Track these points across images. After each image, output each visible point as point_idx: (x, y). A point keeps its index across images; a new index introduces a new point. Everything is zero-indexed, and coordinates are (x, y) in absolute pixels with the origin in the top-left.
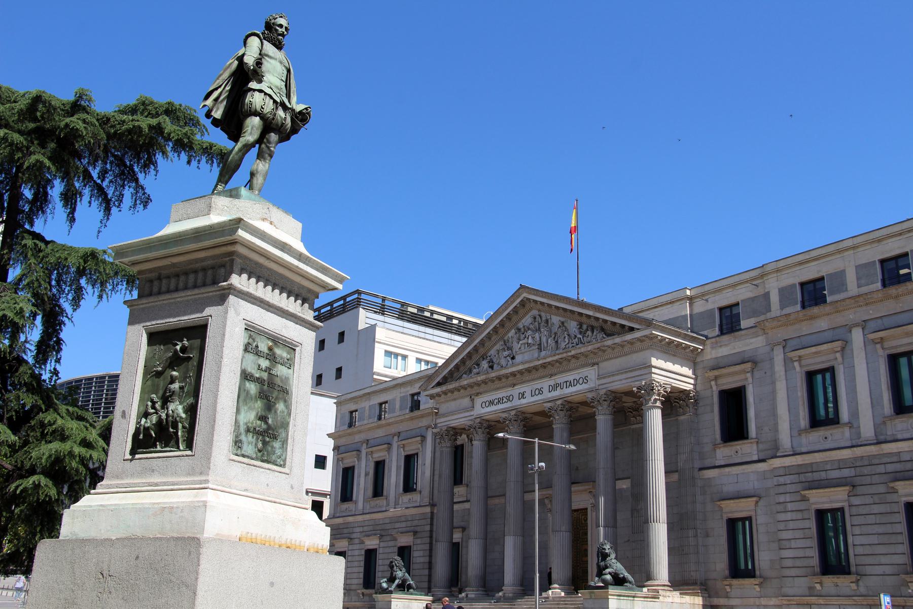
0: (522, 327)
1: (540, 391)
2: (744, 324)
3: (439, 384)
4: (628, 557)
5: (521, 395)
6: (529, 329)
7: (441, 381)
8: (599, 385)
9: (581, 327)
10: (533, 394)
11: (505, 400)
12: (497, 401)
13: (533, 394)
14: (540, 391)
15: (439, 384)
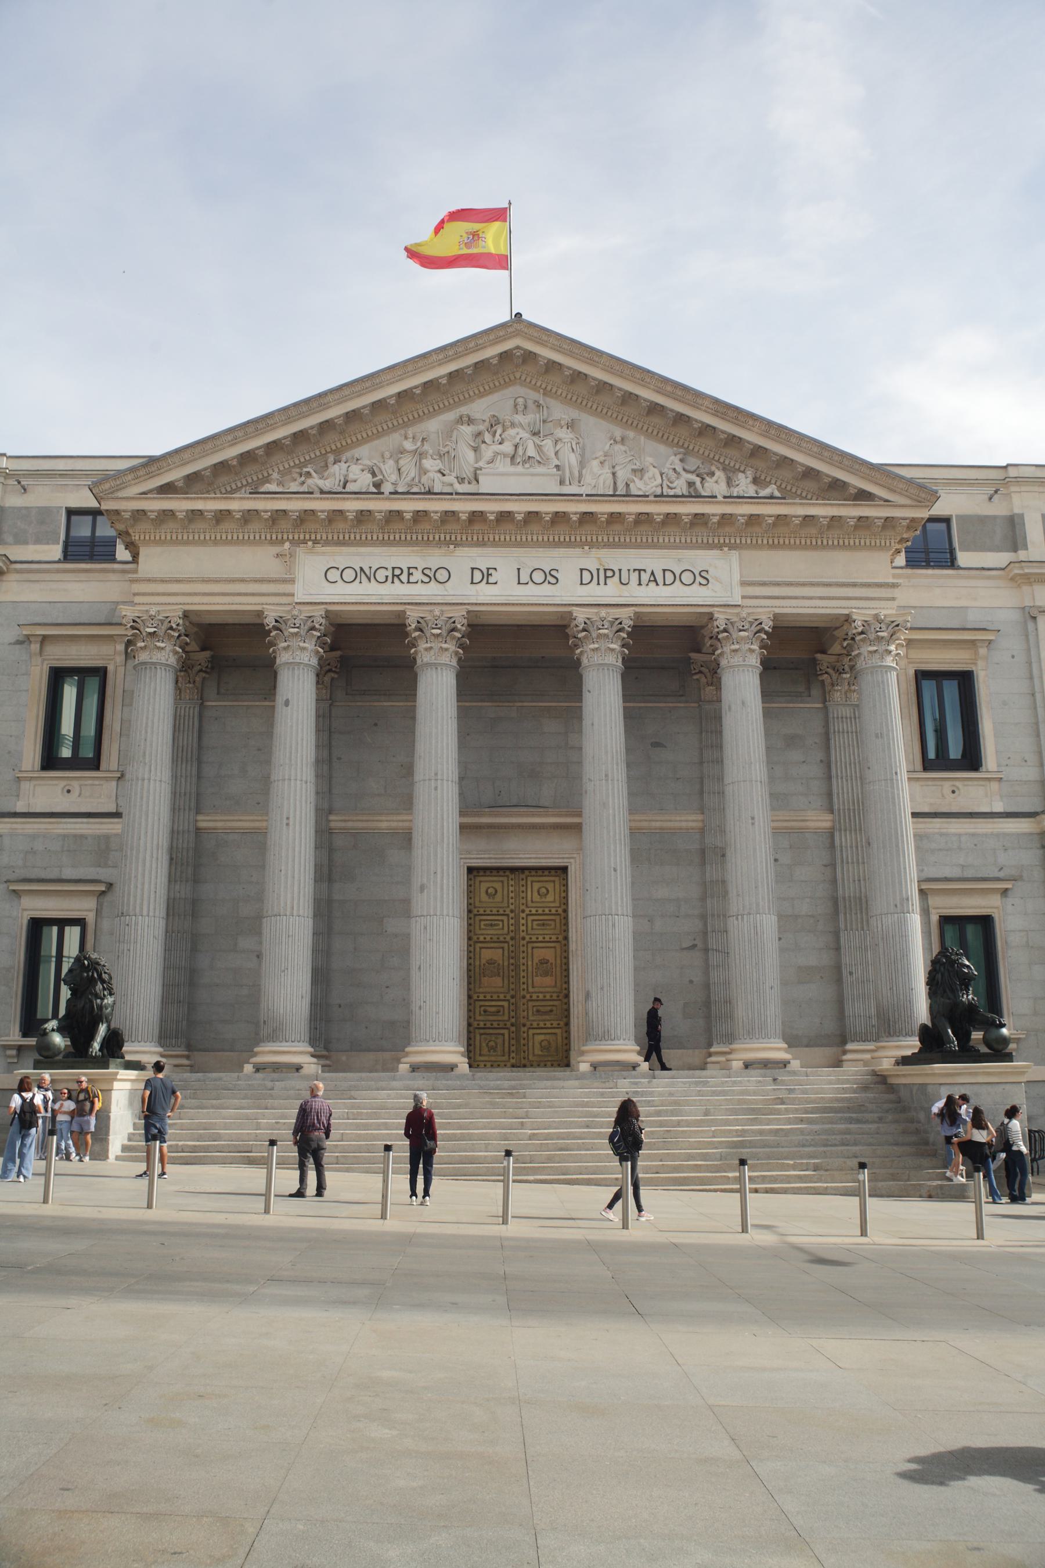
0: (486, 417)
1: (551, 577)
2: (963, 558)
3: (167, 489)
4: (691, 982)
5: (478, 576)
6: (513, 425)
7: (180, 484)
8: (743, 597)
9: (682, 460)
10: (524, 578)
11: (417, 576)
12: (389, 573)
13: (524, 578)
14: (551, 577)
15: (167, 489)
